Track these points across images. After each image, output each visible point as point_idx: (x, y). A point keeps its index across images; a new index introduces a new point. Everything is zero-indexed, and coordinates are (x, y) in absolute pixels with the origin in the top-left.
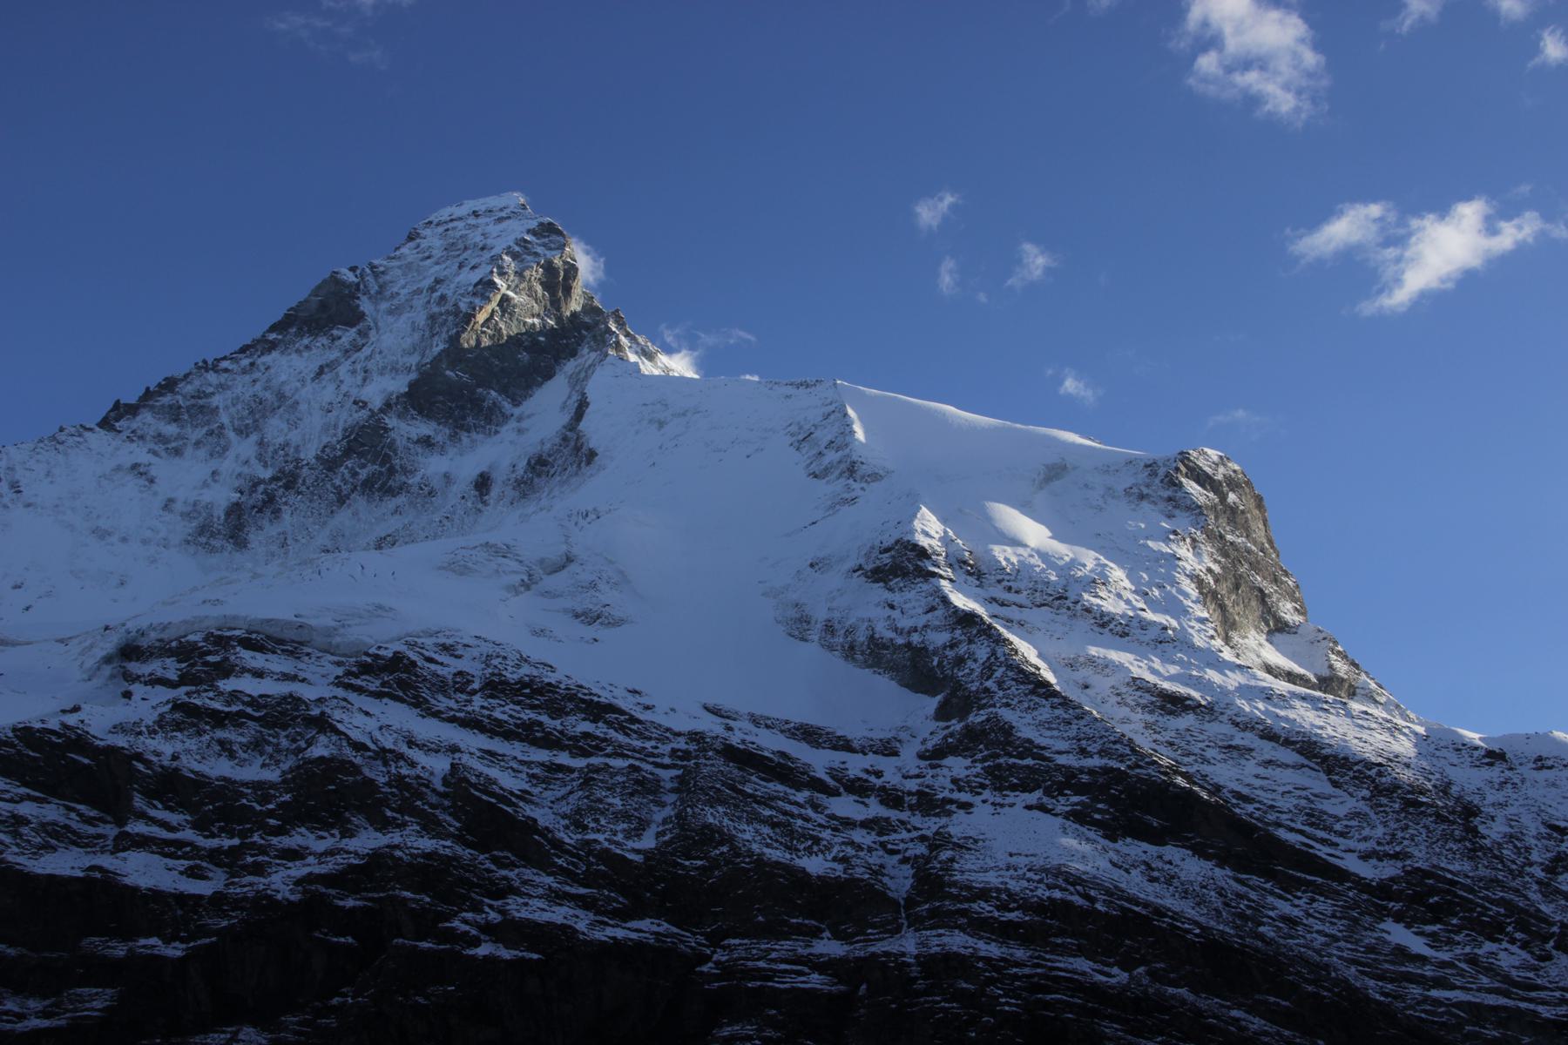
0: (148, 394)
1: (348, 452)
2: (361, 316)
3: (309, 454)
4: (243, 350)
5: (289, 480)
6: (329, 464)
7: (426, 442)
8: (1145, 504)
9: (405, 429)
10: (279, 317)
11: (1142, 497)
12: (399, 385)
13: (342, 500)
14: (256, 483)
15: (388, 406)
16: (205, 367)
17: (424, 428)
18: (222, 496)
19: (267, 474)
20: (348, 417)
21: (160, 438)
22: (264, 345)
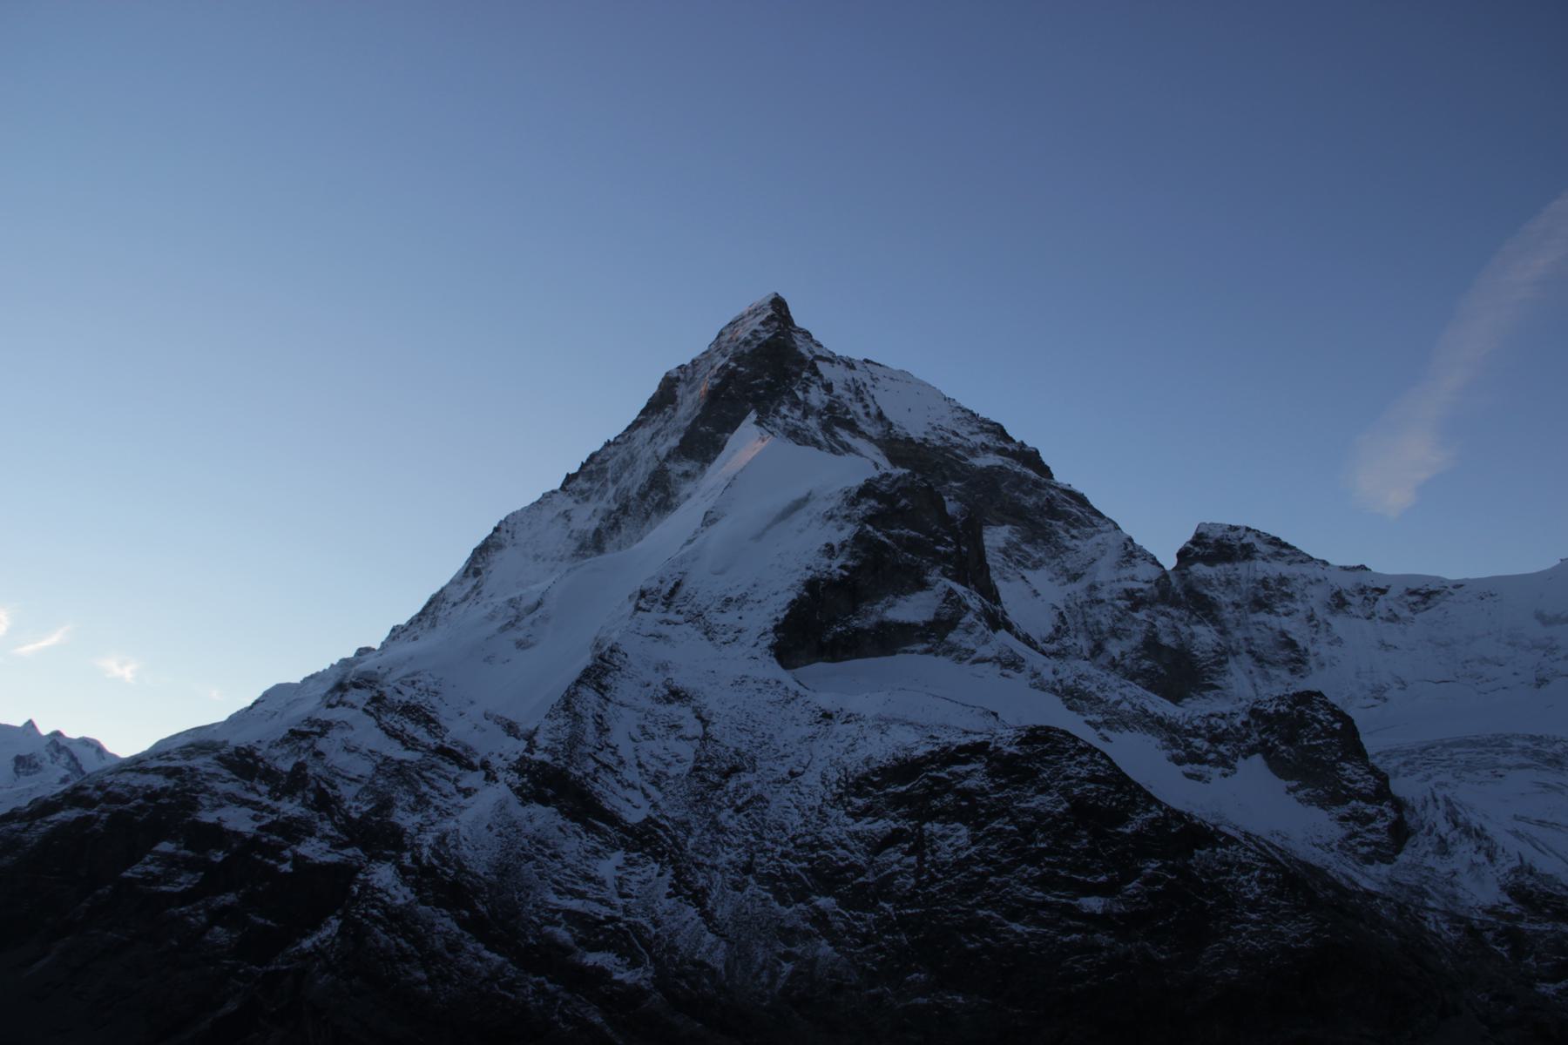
0: (583, 466)
1: (651, 487)
2: (675, 397)
3: (633, 492)
4: (629, 428)
5: (624, 509)
6: (643, 496)
7: (686, 475)
8: (831, 523)
9: (676, 468)
10: (643, 404)
11: (831, 517)
12: (674, 442)
13: (648, 517)
14: (611, 513)
15: (669, 456)
16: (608, 444)
17: (687, 466)
18: (595, 523)
19: (614, 507)
20: (653, 465)
21: (582, 492)
22: (636, 424)
